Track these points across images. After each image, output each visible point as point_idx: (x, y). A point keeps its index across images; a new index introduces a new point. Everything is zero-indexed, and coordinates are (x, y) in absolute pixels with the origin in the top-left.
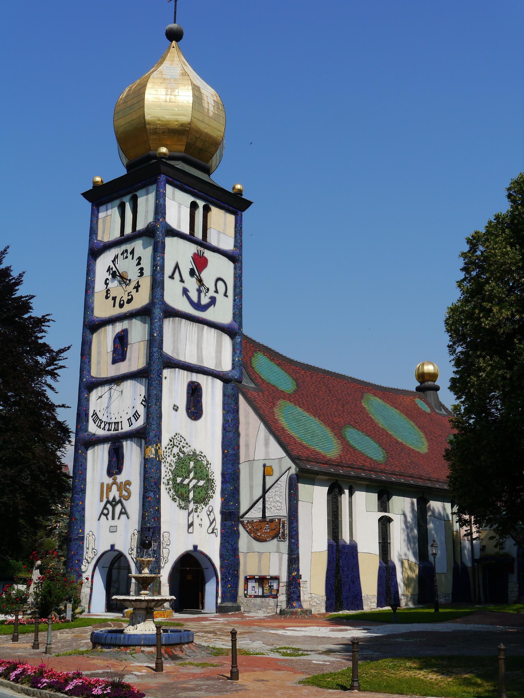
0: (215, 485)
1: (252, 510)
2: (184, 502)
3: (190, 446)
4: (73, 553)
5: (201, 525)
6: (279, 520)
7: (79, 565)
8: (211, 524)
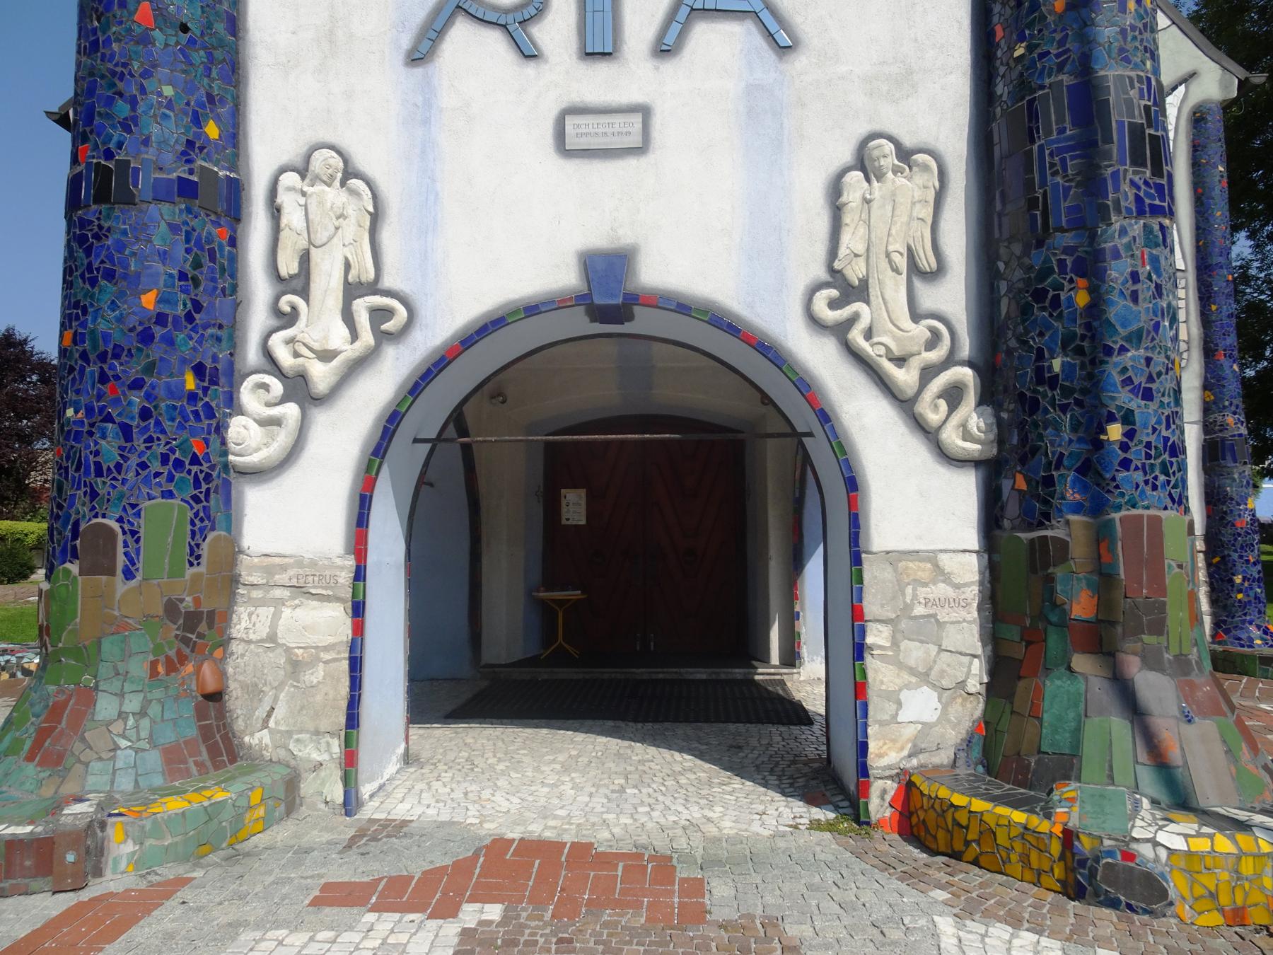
4: (149, 300)
7: (210, 413)
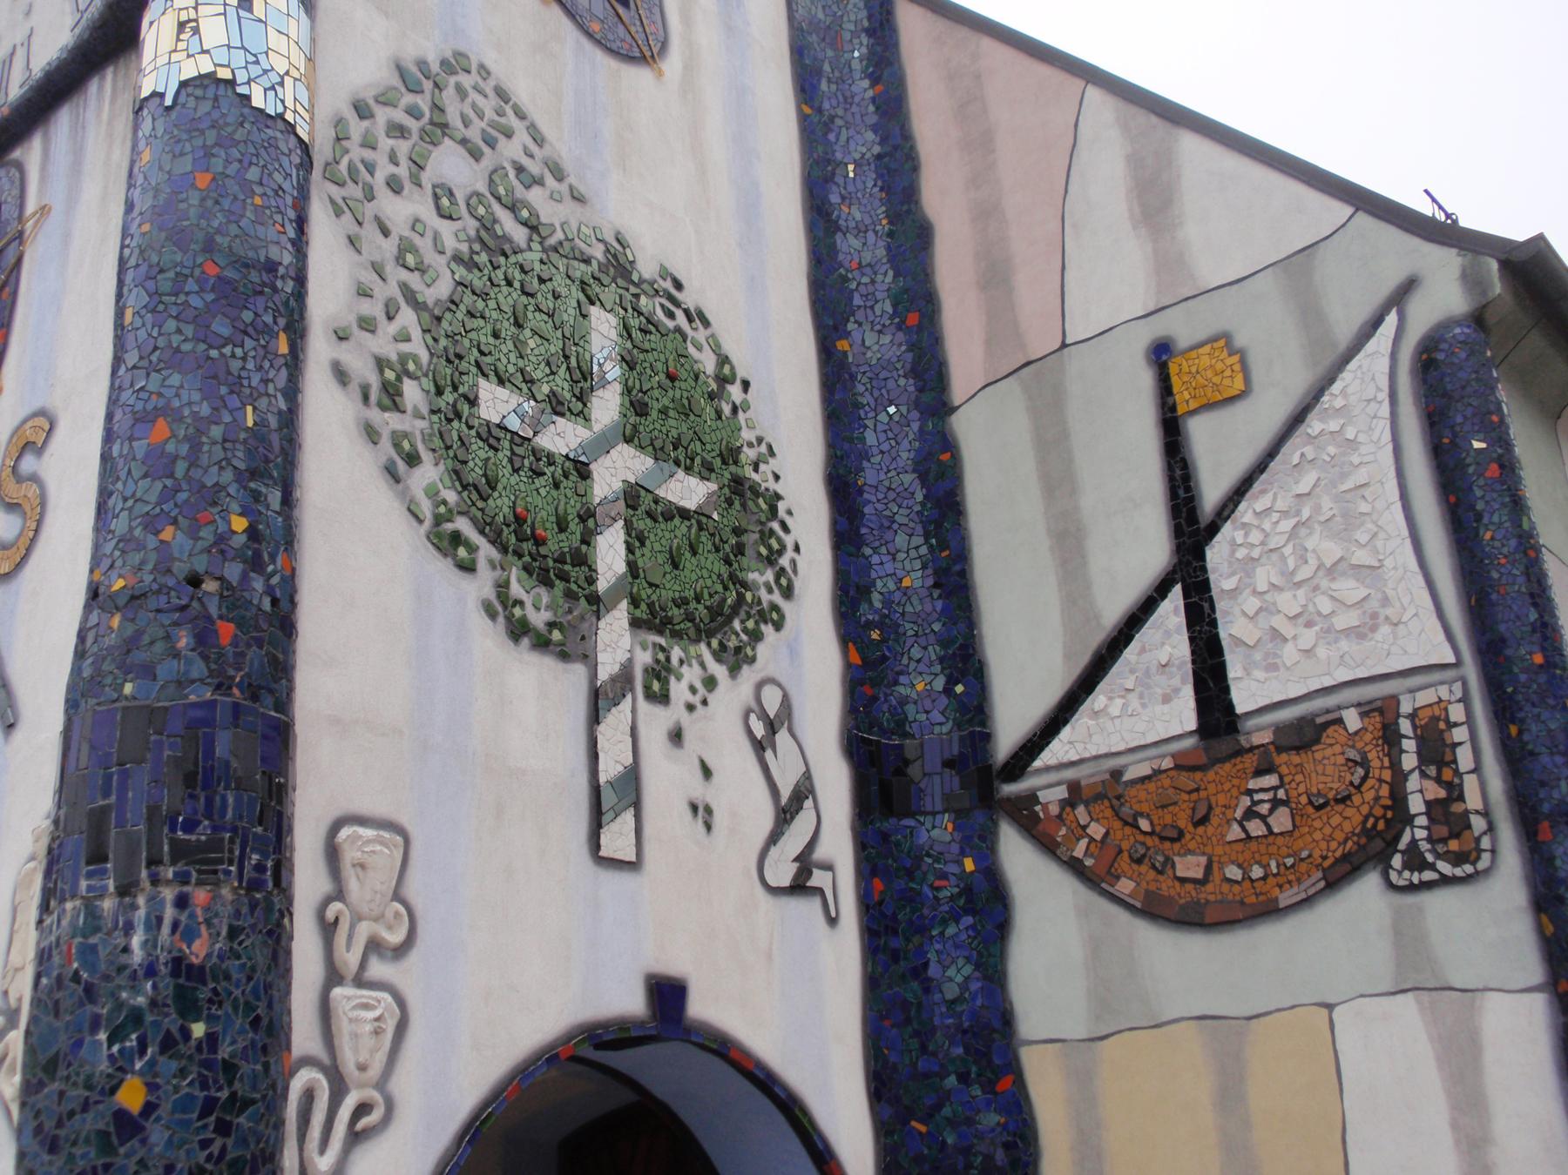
0: (789, 540)
1: (1098, 699)
2: (545, 596)
3: (578, 198)
5: (702, 812)
6: (1383, 713)
8: (785, 815)
